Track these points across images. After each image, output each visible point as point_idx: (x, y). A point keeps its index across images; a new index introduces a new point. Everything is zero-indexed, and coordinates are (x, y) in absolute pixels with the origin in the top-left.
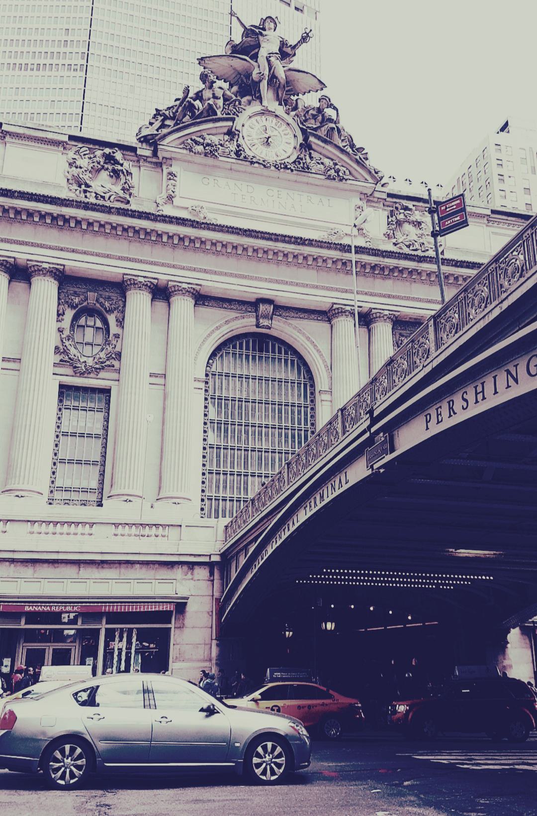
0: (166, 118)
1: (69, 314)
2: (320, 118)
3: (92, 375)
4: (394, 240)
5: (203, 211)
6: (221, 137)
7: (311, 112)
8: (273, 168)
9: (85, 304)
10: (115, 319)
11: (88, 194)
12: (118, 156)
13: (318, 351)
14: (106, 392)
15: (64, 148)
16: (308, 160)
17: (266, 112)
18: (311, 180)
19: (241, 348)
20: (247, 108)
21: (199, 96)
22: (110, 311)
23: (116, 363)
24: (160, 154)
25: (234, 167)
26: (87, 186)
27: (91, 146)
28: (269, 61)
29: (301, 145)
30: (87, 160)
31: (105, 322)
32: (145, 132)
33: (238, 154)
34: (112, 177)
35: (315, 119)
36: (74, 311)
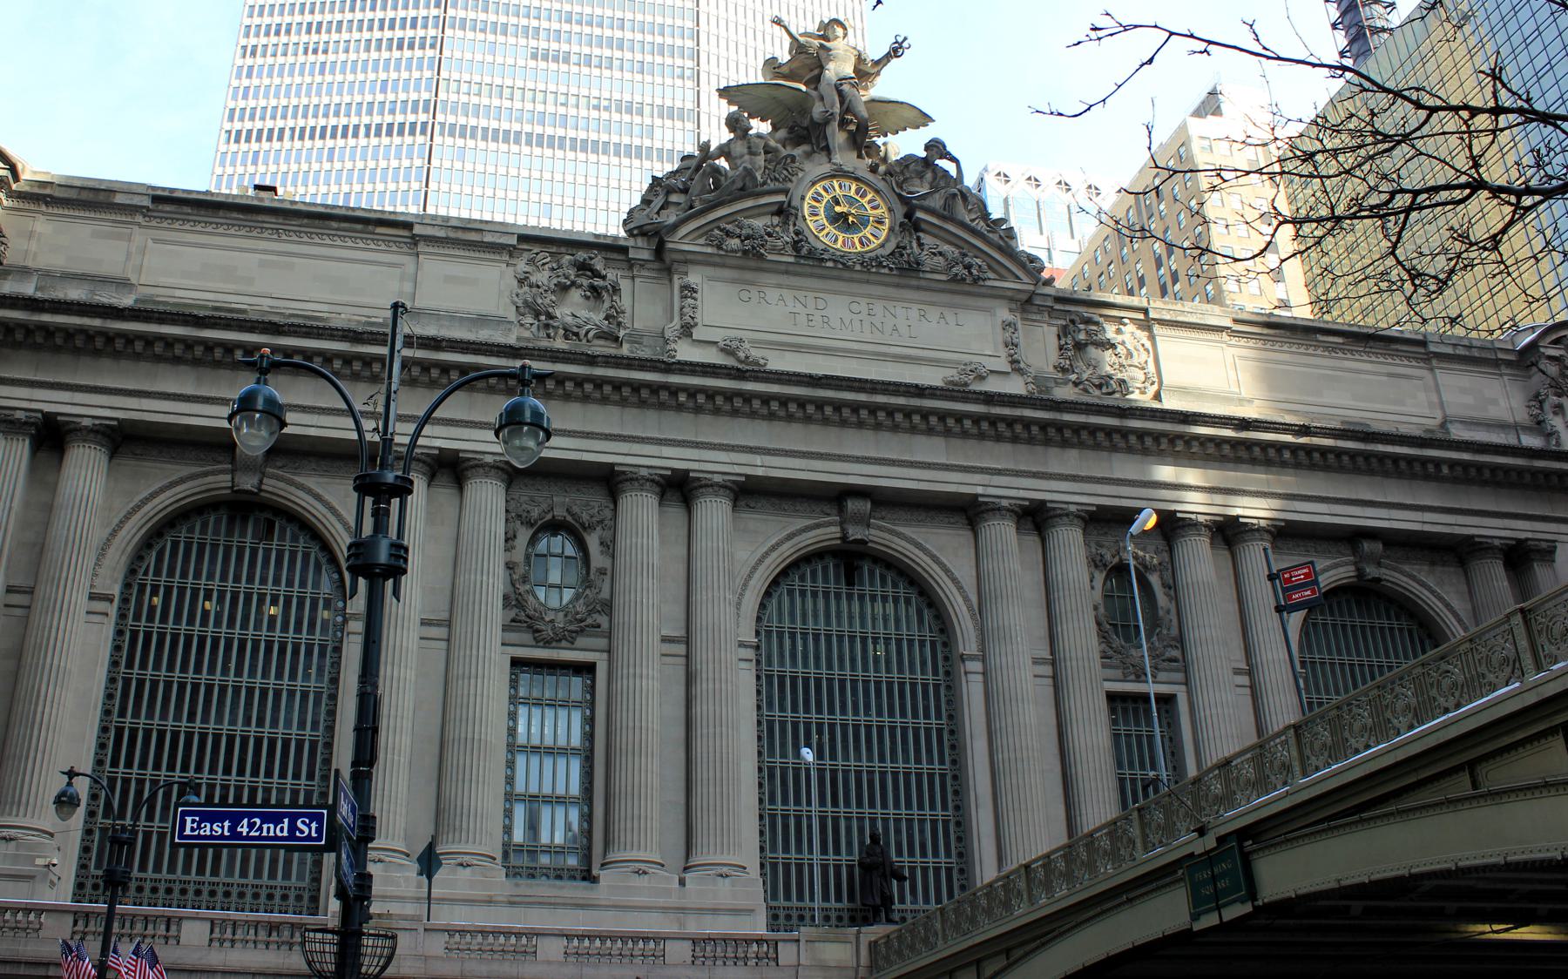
0: (670, 191)
1: (524, 535)
2: (929, 176)
3: (564, 644)
4: (1073, 377)
5: (746, 345)
6: (767, 220)
7: (912, 167)
8: (858, 267)
9: (549, 517)
10: (597, 542)
11: (551, 331)
12: (598, 265)
13: (955, 580)
14: (587, 669)
15: (511, 256)
16: (916, 249)
17: (840, 173)
18: (923, 283)
19: (814, 579)
20: (807, 166)
21: (724, 151)
22: (590, 528)
23: (603, 620)
24: (668, 257)
25: (791, 268)
26: (550, 316)
27: (554, 250)
28: (840, 93)
29: (902, 224)
30: (547, 274)
31: (582, 546)
32: (641, 219)
33: (796, 246)
34: (587, 298)
35: (921, 178)
36: (531, 532)
